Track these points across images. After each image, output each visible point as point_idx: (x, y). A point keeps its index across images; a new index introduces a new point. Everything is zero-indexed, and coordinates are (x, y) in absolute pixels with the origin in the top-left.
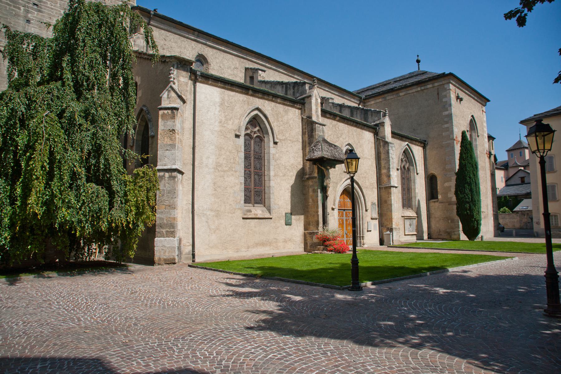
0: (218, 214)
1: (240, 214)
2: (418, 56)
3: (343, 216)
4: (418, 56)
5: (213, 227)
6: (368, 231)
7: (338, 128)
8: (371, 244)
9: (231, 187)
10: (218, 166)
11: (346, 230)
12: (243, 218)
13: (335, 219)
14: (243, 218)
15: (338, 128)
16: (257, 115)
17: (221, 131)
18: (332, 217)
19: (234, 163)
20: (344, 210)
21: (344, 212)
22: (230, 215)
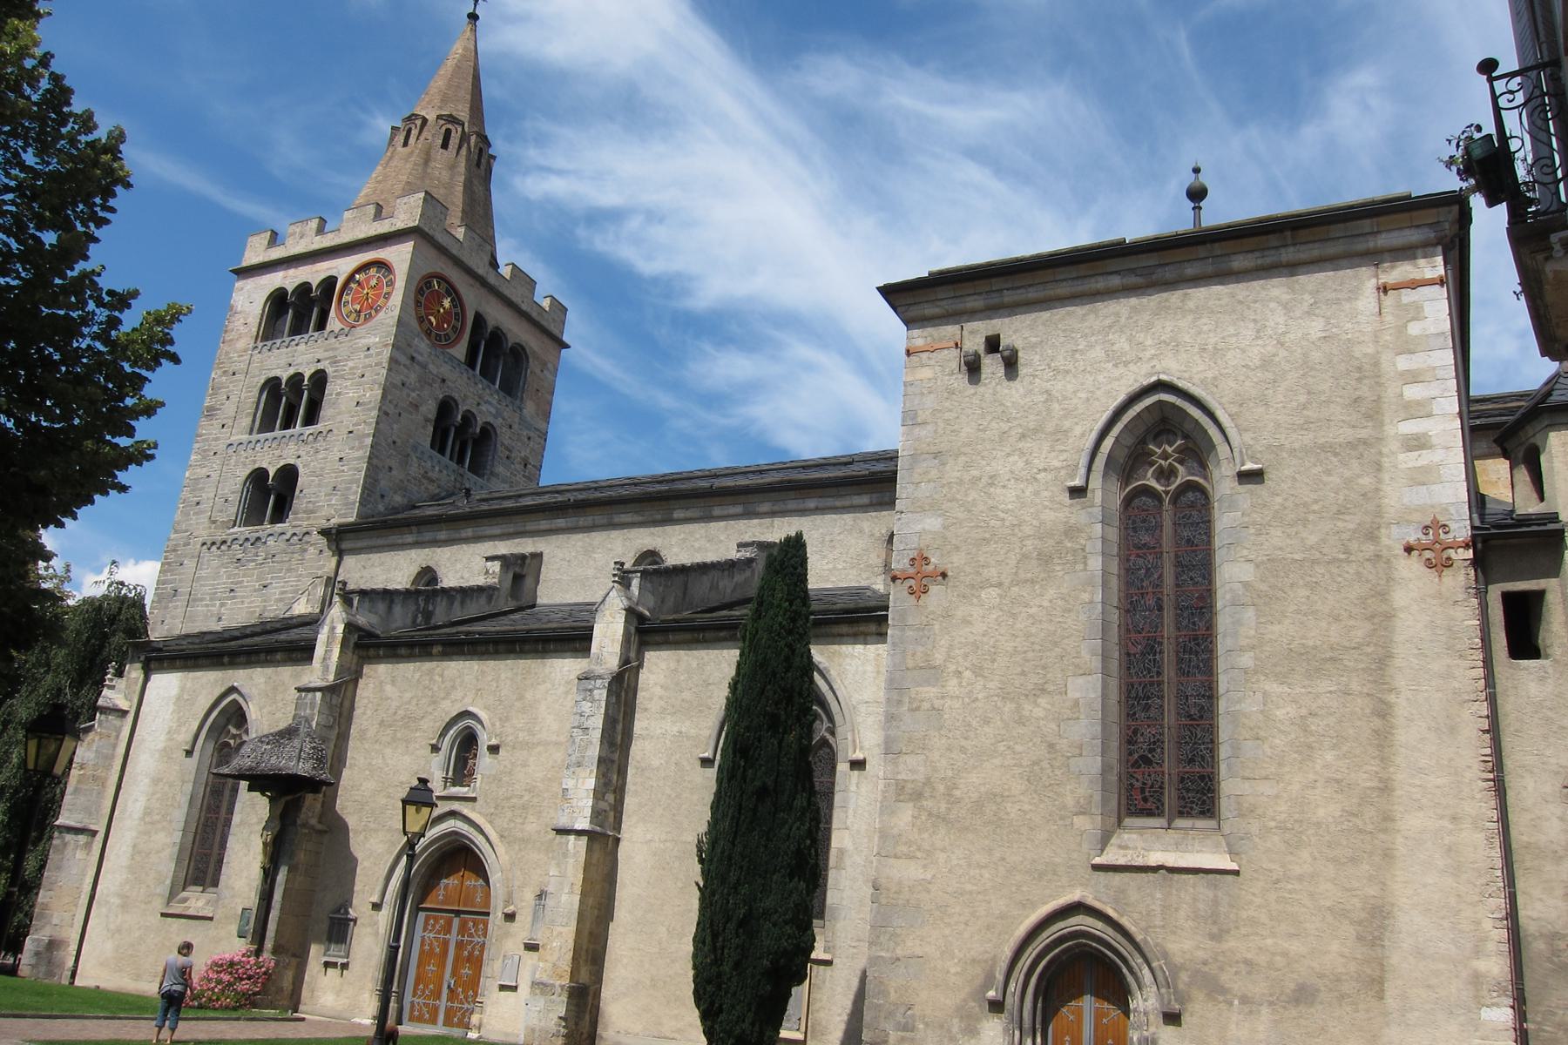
0: (125, 906)
1: (159, 905)
2: (1197, 171)
3: (449, 932)
4: (1197, 171)
5: (112, 927)
6: (503, 988)
7: (442, 676)
8: (507, 1034)
9: (158, 852)
10: (148, 812)
11: (454, 973)
12: (163, 915)
13: (377, 933)
14: (163, 915)
15: (442, 676)
16: (234, 701)
17: (165, 749)
18: (369, 930)
19: (172, 805)
20: (458, 913)
21: (456, 922)
22: (143, 906)
